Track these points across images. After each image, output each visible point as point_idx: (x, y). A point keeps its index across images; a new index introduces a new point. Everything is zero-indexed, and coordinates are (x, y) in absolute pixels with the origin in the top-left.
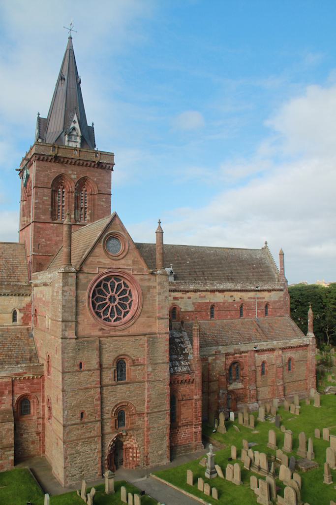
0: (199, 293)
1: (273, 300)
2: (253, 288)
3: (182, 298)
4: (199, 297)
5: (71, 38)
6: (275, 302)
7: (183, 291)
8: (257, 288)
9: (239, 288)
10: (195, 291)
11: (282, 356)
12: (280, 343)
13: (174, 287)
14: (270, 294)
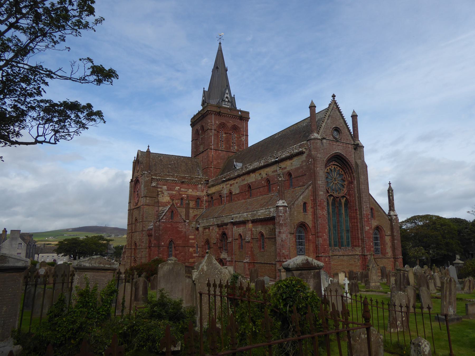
0: (242, 177)
1: (294, 167)
2: (273, 160)
3: (234, 184)
4: (242, 181)
5: (220, 43)
6: (297, 169)
8: (277, 158)
9: (263, 164)
11: (252, 230)
12: (249, 215)
14: (291, 161)
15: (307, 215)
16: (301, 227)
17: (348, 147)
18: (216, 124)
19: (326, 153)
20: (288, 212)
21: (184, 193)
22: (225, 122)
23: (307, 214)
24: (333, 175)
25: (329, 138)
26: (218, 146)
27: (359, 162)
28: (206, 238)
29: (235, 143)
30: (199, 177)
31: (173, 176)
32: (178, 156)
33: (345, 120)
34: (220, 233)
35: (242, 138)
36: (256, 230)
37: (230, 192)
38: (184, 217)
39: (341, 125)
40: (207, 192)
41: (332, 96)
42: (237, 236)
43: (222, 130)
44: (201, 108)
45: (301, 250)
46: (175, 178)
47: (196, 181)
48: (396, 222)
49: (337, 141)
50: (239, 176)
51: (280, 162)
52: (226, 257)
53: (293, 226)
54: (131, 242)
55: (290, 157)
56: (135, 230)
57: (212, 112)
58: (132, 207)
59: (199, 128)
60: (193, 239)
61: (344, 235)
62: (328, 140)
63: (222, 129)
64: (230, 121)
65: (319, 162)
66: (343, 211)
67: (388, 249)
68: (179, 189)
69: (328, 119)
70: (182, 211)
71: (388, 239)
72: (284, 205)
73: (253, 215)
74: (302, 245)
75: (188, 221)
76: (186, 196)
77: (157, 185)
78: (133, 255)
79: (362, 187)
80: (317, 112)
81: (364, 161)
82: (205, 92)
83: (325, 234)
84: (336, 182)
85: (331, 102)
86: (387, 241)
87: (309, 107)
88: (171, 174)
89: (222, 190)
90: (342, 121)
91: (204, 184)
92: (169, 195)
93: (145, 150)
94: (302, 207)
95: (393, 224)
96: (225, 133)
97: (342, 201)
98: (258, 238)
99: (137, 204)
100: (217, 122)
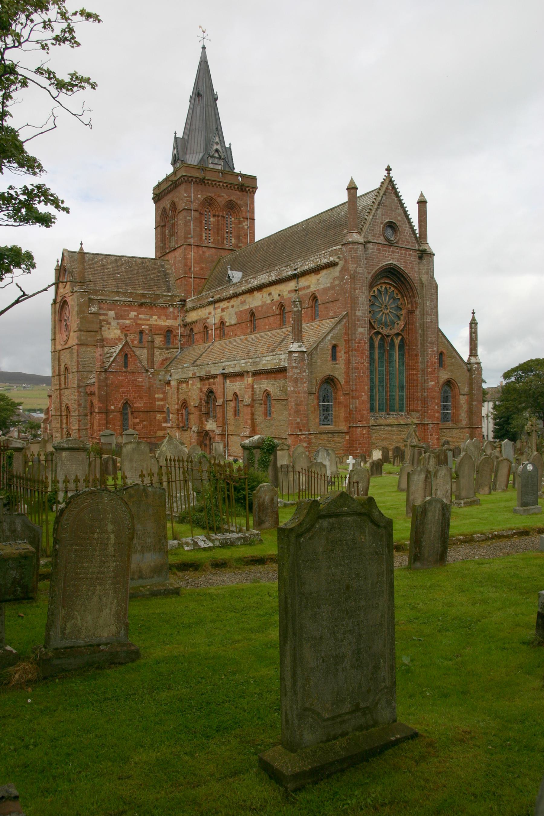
1: (322, 287)
2: (290, 273)
3: (227, 308)
6: (326, 290)
8: (295, 270)
9: (273, 278)
14: (318, 276)
15: (337, 364)
16: (327, 382)
17: (410, 255)
18: (198, 199)
19: (372, 265)
20: (307, 361)
21: (144, 322)
22: (213, 195)
23: (338, 362)
24: (382, 301)
25: (377, 240)
26: (202, 239)
27: (424, 278)
28: (182, 397)
29: (231, 233)
30: (170, 294)
31: (125, 294)
32: (132, 257)
33: (407, 209)
34: (205, 390)
35: (244, 224)
36: (260, 388)
37: (222, 322)
38: (145, 363)
39: (399, 218)
40: (183, 321)
41: (387, 170)
42: (230, 396)
43: (208, 210)
44: (170, 170)
45: (326, 418)
46: (129, 297)
47: (164, 301)
48: (478, 374)
49: (390, 244)
50: (236, 295)
51: (301, 277)
52: (214, 429)
53: (314, 381)
54: (61, 405)
55: (316, 270)
56: (65, 384)
57: (190, 179)
58: (59, 347)
59: (169, 206)
60: (162, 400)
61: (396, 393)
62: (376, 243)
63: (208, 208)
64: (223, 194)
65: (360, 280)
66: (396, 357)
67: (463, 415)
68: (135, 315)
69: (377, 210)
70: (143, 354)
71: (463, 400)
72: (299, 349)
73: (255, 363)
74: (327, 410)
75: (152, 370)
76: (147, 327)
77: (98, 310)
78: (64, 426)
79: (429, 319)
80: (358, 195)
81: (432, 277)
82: (179, 141)
83: (363, 394)
84: (388, 311)
85: (384, 179)
86: (462, 402)
87: (347, 189)
88: (121, 290)
89: (208, 318)
90: (400, 211)
91: (178, 306)
92: (118, 327)
93: (77, 250)
94: (330, 352)
95: (473, 376)
96: (214, 216)
97: (396, 341)
98: (262, 400)
99: (66, 342)
100: (199, 196)
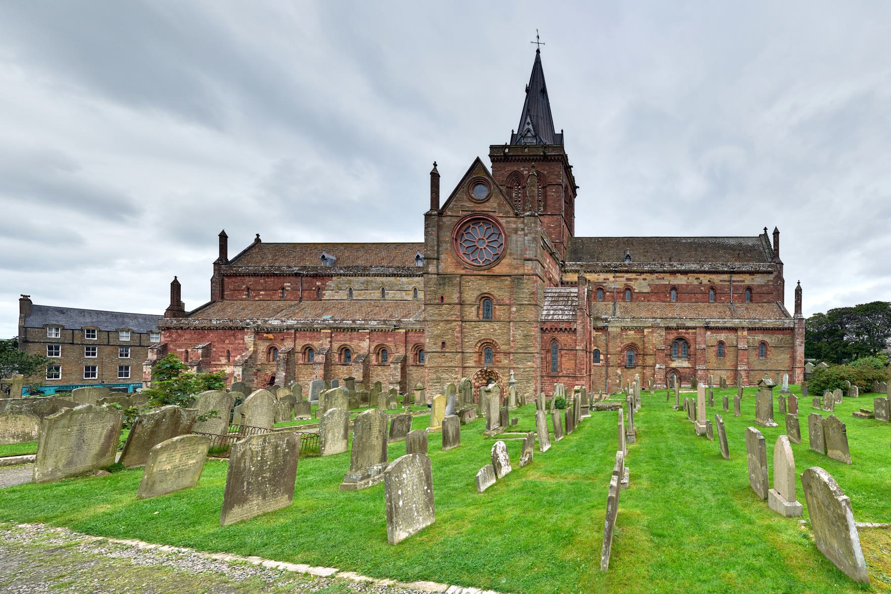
2: (726, 269)
3: (636, 279)
7: (636, 272)
9: (707, 269)
10: (652, 272)
13: (626, 268)
14: (753, 277)
28: (627, 342)
